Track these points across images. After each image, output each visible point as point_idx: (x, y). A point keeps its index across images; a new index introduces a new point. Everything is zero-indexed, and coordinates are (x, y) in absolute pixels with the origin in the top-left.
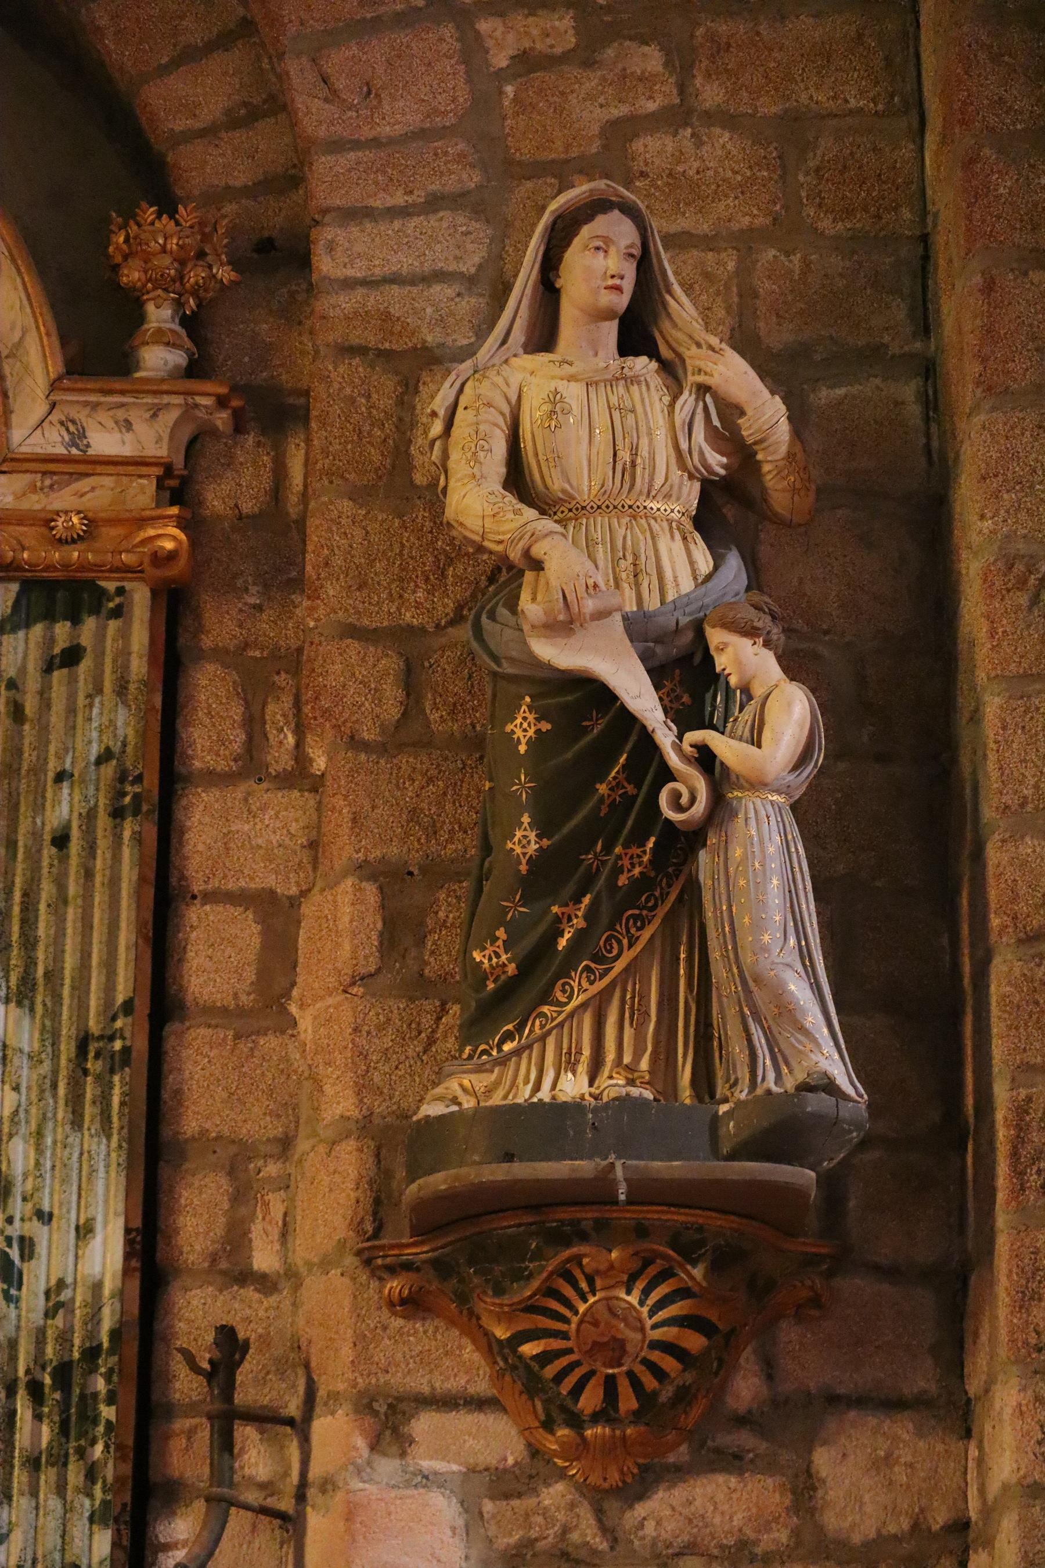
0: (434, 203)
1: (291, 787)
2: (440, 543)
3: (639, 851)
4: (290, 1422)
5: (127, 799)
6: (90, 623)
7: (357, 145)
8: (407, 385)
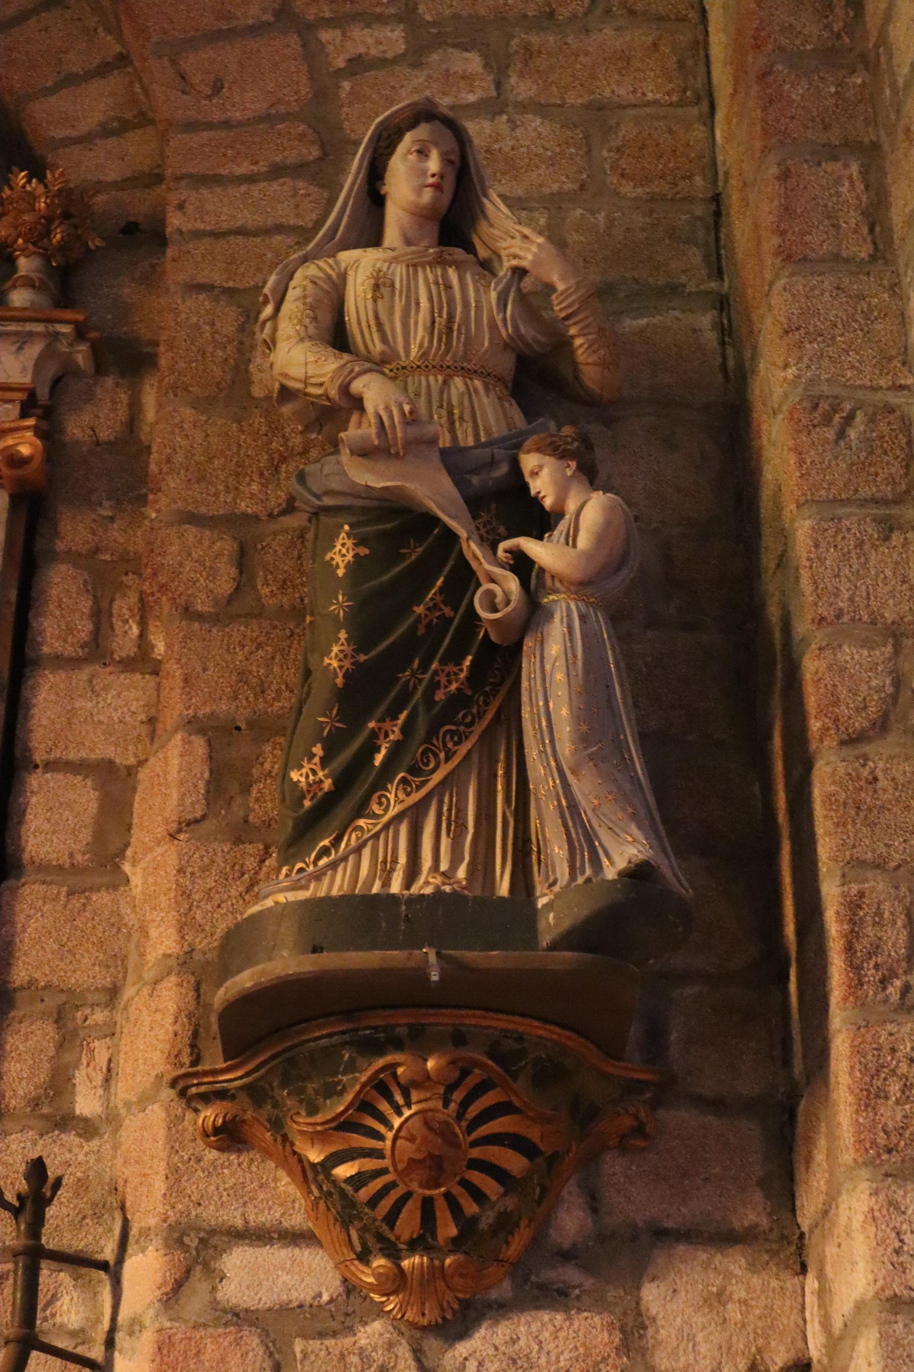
0: (277, 172)
1: (133, 671)
2: (274, 444)
3: (455, 669)
4: (103, 1266)
7: (210, 126)
8: (248, 317)
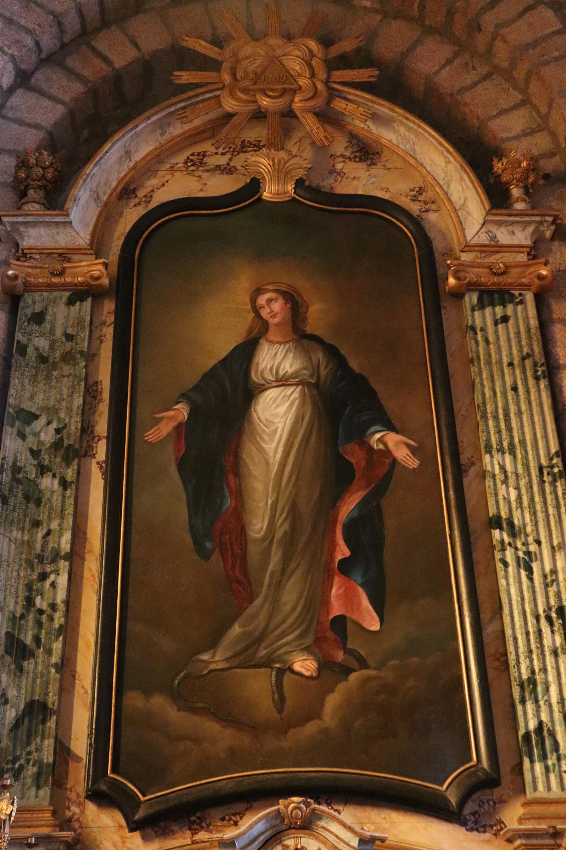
5: (539, 373)
6: (510, 307)
